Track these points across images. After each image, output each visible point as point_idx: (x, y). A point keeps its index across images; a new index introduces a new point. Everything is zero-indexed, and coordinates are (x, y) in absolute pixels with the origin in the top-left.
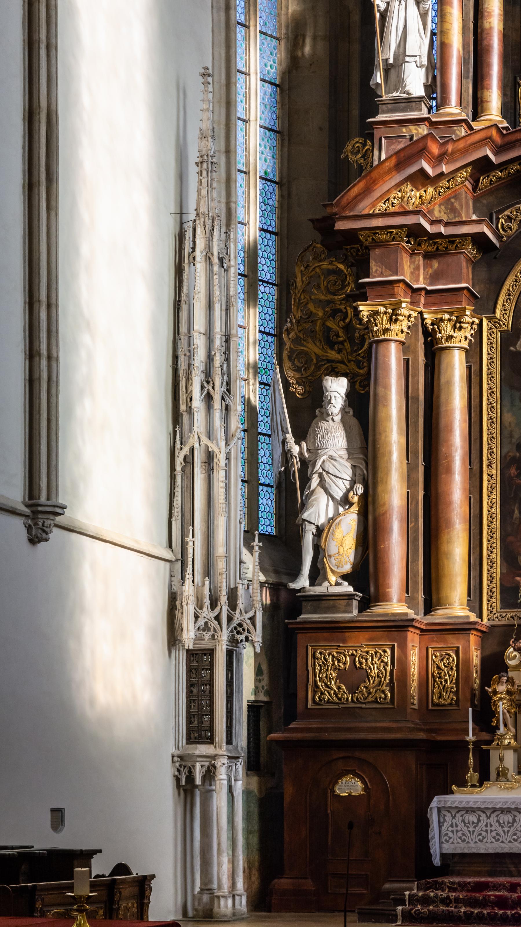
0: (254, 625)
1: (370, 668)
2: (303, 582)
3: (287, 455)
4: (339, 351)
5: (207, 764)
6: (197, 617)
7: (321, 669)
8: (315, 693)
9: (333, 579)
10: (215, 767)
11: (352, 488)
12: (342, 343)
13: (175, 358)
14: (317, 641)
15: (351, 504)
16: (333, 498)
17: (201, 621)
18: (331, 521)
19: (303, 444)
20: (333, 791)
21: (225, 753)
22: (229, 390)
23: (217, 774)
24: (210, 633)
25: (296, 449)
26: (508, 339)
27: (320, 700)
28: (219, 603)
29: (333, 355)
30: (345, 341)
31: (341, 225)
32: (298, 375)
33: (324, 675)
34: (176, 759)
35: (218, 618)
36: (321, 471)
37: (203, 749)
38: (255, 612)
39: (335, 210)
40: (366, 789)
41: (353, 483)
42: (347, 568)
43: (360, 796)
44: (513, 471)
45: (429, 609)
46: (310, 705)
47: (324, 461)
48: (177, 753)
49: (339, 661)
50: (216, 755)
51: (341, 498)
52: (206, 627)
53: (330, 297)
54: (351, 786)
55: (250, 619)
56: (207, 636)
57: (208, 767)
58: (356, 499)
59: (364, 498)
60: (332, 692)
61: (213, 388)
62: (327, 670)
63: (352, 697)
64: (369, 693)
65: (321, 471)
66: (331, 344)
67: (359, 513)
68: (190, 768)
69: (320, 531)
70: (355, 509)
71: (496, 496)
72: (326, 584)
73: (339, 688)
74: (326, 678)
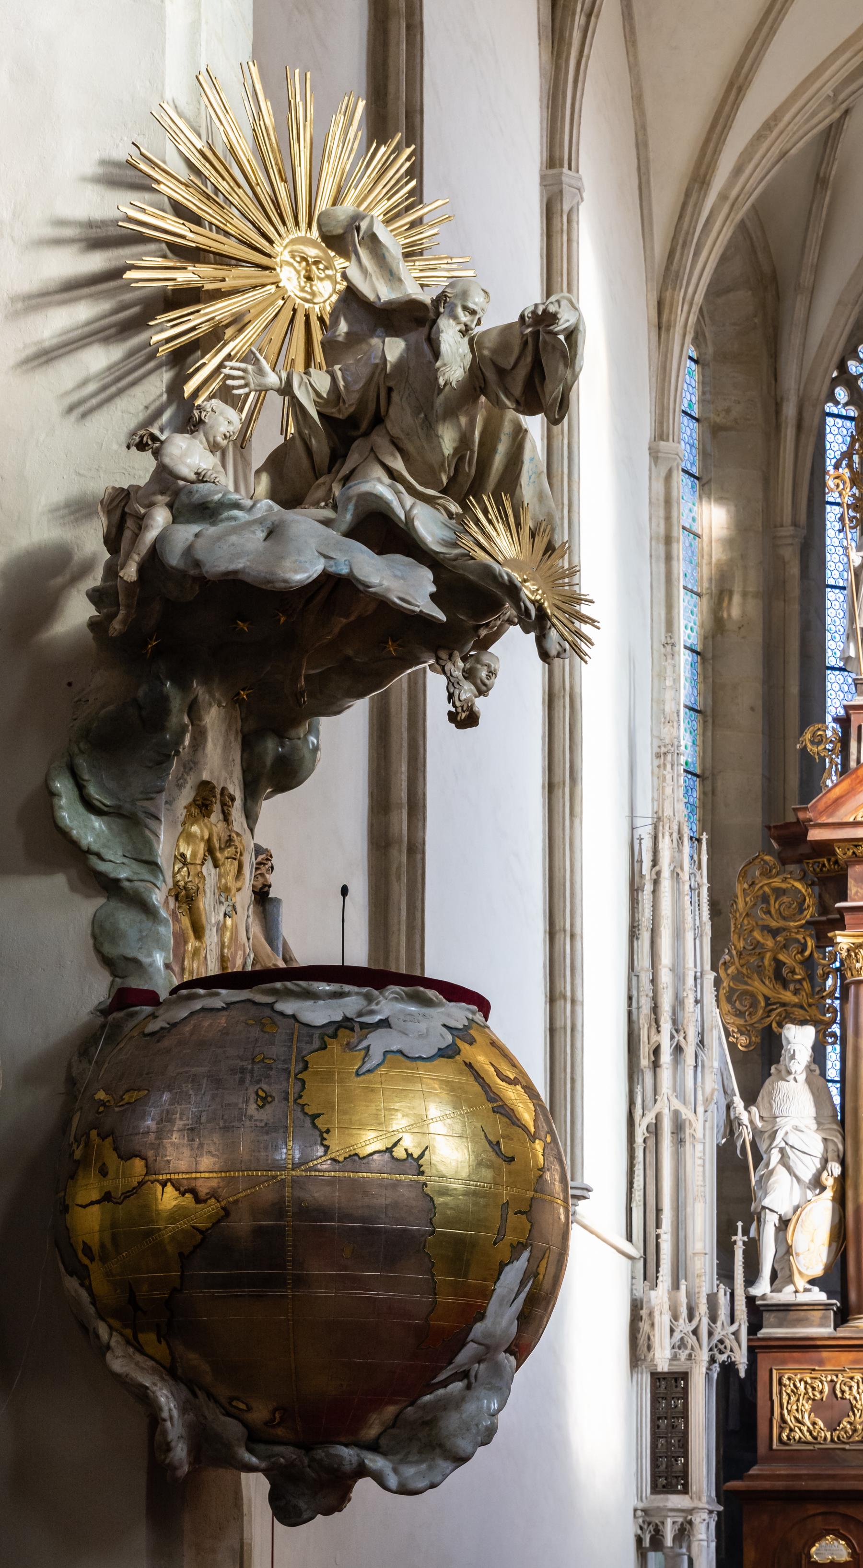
0: (738, 1340)
1: (855, 1398)
2: (762, 1288)
3: (731, 1126)
4: (796, 992)
5: (680, 1520)
6: (672, 1331)
7: (789, 1399)
8: (781, 1429)
9: (801, 1283)
10: (690, 1523)
11: (824, 1167)
12: (800, 981)
13: (630, 998)
14: (784, 1362)
15: (823, 1188)
16: (798, 1179)
17: (677, 1336)
19: (754, 1109)
20: (809, 1556)
21: (707, 1506)
22: (702, 1042)
23: (695, 1532)
24: (687, 1352)
25: (745, 1117)
27: (789, 1439)
28: (697, 1314)
29: (788, 996)
30: (803, 979)
31: (815, 835)
32: (741, 1022)
33: (795, 1407)
34: (639, 1513)
35: (695, 1332)
36: (783, 1144)
37: (676, 1501)
38: (740, 1326)
39: (810, 815)
40: (853, 1554)
41: (825, 1161)
42: (817, 1270)
43: (846, 1563)
46: (775, 1446)
47: (787, 1133)
48: (640, 1505)
49: (813, 1389)
50: (694, 1509)
51: (810, 1181)
52: (682, 1344)
53: (782, 923)
55: (733, 1334)
56: (683, 1355)
57: (682, 1524)
58: (829, 1182)
60: (805, 1429)
61: (685, 1038)
62: (798, 1400)
63: (832, 1435)
64: (855, 1431)
65: (783, 1144)
66: (785, 984)
67: (834, 1200)
68: (657, 1525)
69: (784, 1224)
70: (829, 1194)
72: (790, 1288)
73: (814, 1424)
74: (797, 1410)
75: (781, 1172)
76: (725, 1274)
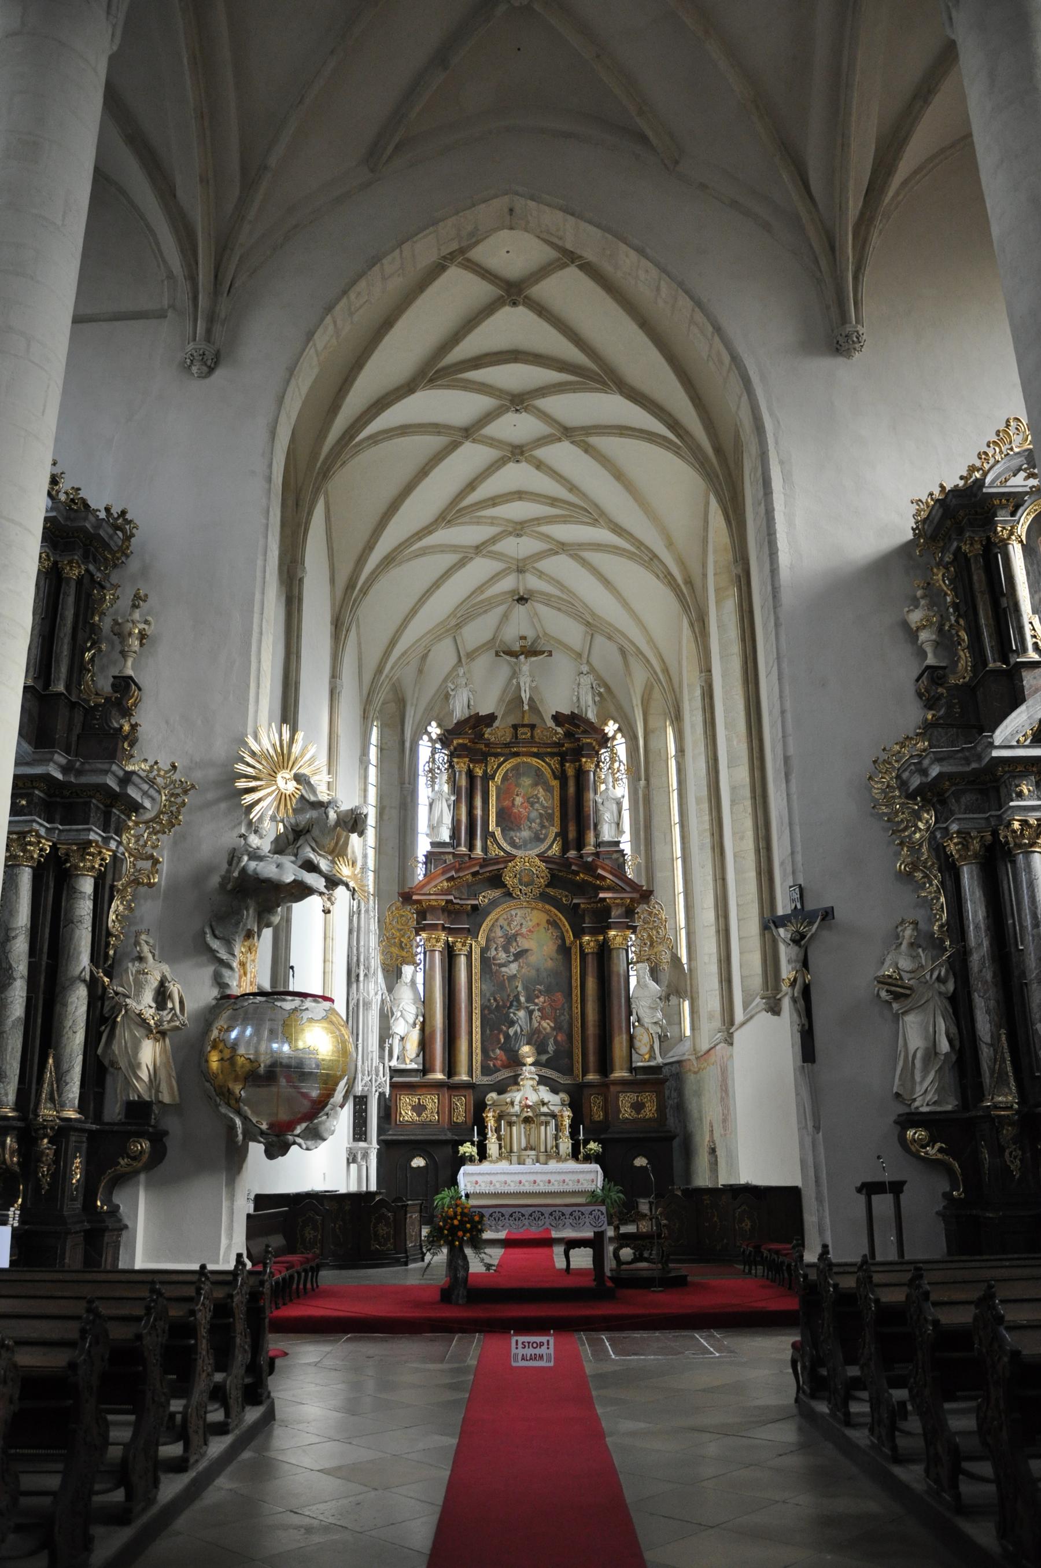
18: (408, 1033)
26: (484, 951)
41: (417, 1016)
44: (486, 1012)
45: (449, 1077)
54: (418, 1162)
59: (423, 1023)
66: (403, 949)
70: (418, 1027)
71: (479, 1023)
75: (401, 1019)
76: (381, 1058)
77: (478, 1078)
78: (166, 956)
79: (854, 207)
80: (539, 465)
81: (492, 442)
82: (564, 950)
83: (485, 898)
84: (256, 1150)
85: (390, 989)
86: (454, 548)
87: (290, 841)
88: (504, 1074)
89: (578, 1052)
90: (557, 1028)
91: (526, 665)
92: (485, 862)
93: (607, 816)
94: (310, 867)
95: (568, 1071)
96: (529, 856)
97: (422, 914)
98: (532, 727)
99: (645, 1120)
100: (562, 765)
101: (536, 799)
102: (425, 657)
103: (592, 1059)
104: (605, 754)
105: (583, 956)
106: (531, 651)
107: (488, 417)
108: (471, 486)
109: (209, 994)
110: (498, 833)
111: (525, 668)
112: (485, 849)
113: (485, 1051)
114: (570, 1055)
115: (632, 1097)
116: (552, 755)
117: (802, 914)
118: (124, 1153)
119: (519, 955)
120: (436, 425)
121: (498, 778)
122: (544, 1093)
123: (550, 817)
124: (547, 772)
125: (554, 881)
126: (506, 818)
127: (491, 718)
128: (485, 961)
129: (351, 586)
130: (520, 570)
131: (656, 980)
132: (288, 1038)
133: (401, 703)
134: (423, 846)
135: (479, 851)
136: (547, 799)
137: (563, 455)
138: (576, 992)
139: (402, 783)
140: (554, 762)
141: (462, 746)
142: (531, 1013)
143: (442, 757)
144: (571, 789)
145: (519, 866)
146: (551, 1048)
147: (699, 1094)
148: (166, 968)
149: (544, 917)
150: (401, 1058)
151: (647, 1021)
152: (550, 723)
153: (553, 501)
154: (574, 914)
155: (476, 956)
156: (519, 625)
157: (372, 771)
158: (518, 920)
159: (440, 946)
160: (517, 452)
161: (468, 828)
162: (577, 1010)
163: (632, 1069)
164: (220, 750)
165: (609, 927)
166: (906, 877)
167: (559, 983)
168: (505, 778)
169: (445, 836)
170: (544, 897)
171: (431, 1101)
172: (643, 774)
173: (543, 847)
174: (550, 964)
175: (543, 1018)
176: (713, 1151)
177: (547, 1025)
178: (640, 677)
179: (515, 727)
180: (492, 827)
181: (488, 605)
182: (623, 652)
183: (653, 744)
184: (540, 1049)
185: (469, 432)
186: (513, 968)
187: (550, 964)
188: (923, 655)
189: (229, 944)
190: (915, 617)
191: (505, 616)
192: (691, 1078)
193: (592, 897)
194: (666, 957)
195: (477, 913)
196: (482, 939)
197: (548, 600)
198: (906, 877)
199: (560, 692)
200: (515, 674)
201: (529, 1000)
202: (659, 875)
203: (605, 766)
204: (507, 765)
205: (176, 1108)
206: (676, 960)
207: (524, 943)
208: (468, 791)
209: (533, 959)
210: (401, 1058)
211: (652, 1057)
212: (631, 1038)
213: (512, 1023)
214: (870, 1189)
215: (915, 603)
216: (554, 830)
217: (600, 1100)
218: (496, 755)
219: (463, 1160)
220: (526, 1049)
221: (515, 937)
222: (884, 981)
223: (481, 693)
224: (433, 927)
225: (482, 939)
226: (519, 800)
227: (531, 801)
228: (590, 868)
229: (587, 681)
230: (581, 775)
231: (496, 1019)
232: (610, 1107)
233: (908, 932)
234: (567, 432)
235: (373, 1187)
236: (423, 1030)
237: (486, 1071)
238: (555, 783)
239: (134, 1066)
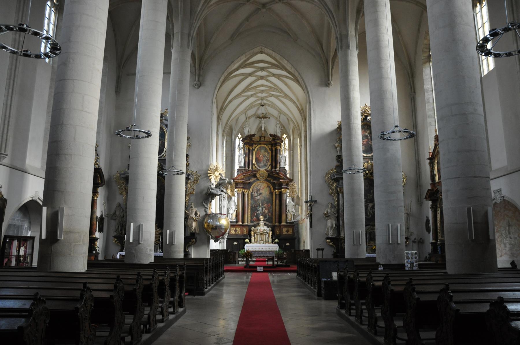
26: (251, 193)
54: (235, 243)
77: (250, 224)
78: (196, 207)
79: (332, 55)
80: (267, 80)
81: (256, 76)
82: (271, 193)
83: (251, 180)
84: (212, 241)
85: (229, 202)
86: (246, 96)
87: (218, 186)
88: (256, 223)
89: (274, 218)
90: (269, 212)
91: (263, 121)
92: (252, 172)
93: (282, 161)
94: (222, 191)
95: (271, 222)
96: (263, 170)
97: (237, 184)
98: (265, 137)
99: (289, 235)
100: (272, 147)
101: (265, 155)
102: (238, 119)
103: (277, 220)
104: (283, 144)
105: (276, 195)
106: (265, 117)
107: (255, 72)
108: (251, 84)
109: (203, 213)
110: (255, 164)
111: (263, 122)
112: (252, 168)
113: (251, 217)
114: (272, 219)
115: (286, 229)
116: (269, 144)
117: (311, 201)
118: (191, 241)
119: (260, 194)
120: (243, 74)
121: (256, 150)
122: (265, 228)
123: (268, 160)
124: (268, 149)
125: (269, 176)
126: (257, 160)
127: (254, 135)
128: (252, 195)
129: (221, 109)
130: (262, 100)
131: (293, 201)
132: (219, 222)
133: (231, 129)
134: (237, 167)
135: (251, 169)
136: (268, 155)
137: (273, 79)
138: (274, 203)
139: (232, 150)
140: (270, 146)
141: (247, 142)
142: (263, 208)
143: (242, 144)
144: (274, 154)
145: (260, 172)
146: (267, 217)
147: (302, 229)
148: (196, 209)
149: (266, 185)
150: (232, 219)
151: (290, 211)
152: (269, 136)
153: (270, 87)
154: (274, 185)
155: (250, 194)
156: (262, 110)
157: (225, 148)
158: (260, 186)
159: (241, 192)
160: (262, 78)
161: (248, 163)
162: (274, 208)
163: (286, 222)
164: (204, 168)
165: (282, 188)
166: (331, 194)
167: (269, 201)
168: (257, 150)
169: (242, 165)
170: (266, 180)
171: (238, 229)
172: (292, 149)
173: (266, 168)
174: (267, 196)
175: (266, 209)
176: (304, 242)
177: (266, 211)
178: (292, 125)
179: (260, 137)
180: (254, 162)
181: (254, 106)
182: (288, 119)
183: (295, 142)
184: (265, 217)
185: (250, 75)
186: (259, 197)
187: (267, 196)
188: (337, 152)
189: (207, 204)
190: (337, 145)
191: (258, 108)
192: (300, 225)
193: (277, 180)
194: (295, 196)
195: (250, 184)
196: (251, 190)
197: (269, 105)
198: (331, 194)
199: (272, 128)
200: (260, 123)
201: (262, 205)
202: (295, 175)
203: (282, 147)
204: (258, 147)
205: (198, 234)
206: (298, 196)
207: (261, 191)
208: (248, 153)
209: (263, 195)
210: (232, 219)
211: (291, 220)
212: (286, 215)
213: (258, 211)
214: (318, 250)
215: (337, 142)
216: (269, 163)
217: (279, 229)
218: (255, 144)
219: (246, 243)
220: (261, 217)
221: (259, 190)
222: (325, 214)
223: (251, 129)
224: (240, 187)
225: (251, 190)
226: (261, 156)
227: (264, 156)
228: (278, 174)
229: (278, 126)
230: (276, 150)
231: (254, 209)
232: (281, 231)
233: (330, 205)
234: (274, 75)
235: (225, 249)
236: (237, 212)
237: (251, 222)
238: (270, 152)
239: (192, 226)
